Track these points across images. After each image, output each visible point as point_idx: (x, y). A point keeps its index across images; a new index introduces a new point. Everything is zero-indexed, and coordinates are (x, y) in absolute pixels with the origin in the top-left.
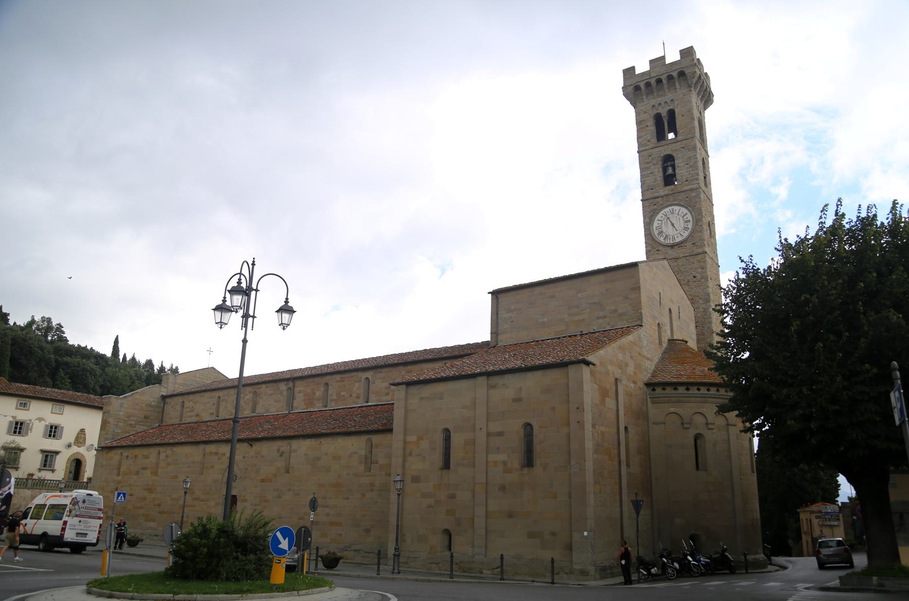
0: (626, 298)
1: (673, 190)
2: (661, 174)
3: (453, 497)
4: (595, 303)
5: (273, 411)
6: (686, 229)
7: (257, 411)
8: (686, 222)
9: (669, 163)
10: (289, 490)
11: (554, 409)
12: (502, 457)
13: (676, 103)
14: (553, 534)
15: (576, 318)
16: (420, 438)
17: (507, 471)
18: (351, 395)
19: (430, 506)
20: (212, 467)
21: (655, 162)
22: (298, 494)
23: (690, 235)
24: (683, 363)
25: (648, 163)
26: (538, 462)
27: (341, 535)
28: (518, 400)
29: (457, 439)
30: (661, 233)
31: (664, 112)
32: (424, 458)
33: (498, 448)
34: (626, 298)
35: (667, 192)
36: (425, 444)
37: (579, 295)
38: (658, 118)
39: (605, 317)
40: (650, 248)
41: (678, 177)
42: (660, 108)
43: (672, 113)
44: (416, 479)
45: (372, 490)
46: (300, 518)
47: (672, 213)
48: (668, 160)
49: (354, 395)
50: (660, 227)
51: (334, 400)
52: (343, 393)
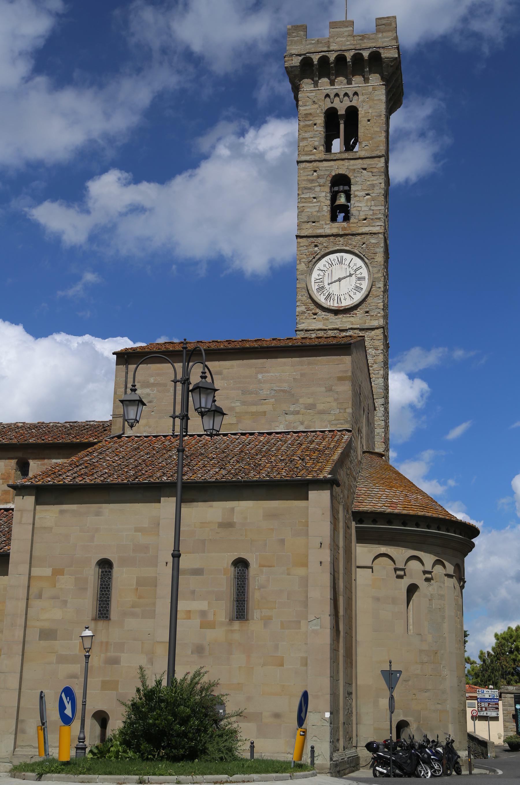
0: (330, 389)
1: (344, 229)
2: (328, 202)
3: (115, 661)
4: (284, 391)
6: (358, 289)
8: (359, 279)
9: (341, 188)
12: (203, 605)
13: (361, 98)
14: (277, 716)
15: (253, 409)
16: (58, 572)
17: (206, 625)
21: (322, 181)
24: (391, 487)
25: (312, 181)
26: (256, 613)
28: (227, 525)
29: (121, 576)
30: (321, 289)
31: (342, 108)
32: (65, 602)
33: (193, 592)
34: (330, 389)
35: (335, 231)
36: (66, 582)
37: (260, 376)
38: (331, 116)
39: (298, 413)
42: (337, 99)
44: (47, 634)
47: (341, 262)
48: (341, 183)
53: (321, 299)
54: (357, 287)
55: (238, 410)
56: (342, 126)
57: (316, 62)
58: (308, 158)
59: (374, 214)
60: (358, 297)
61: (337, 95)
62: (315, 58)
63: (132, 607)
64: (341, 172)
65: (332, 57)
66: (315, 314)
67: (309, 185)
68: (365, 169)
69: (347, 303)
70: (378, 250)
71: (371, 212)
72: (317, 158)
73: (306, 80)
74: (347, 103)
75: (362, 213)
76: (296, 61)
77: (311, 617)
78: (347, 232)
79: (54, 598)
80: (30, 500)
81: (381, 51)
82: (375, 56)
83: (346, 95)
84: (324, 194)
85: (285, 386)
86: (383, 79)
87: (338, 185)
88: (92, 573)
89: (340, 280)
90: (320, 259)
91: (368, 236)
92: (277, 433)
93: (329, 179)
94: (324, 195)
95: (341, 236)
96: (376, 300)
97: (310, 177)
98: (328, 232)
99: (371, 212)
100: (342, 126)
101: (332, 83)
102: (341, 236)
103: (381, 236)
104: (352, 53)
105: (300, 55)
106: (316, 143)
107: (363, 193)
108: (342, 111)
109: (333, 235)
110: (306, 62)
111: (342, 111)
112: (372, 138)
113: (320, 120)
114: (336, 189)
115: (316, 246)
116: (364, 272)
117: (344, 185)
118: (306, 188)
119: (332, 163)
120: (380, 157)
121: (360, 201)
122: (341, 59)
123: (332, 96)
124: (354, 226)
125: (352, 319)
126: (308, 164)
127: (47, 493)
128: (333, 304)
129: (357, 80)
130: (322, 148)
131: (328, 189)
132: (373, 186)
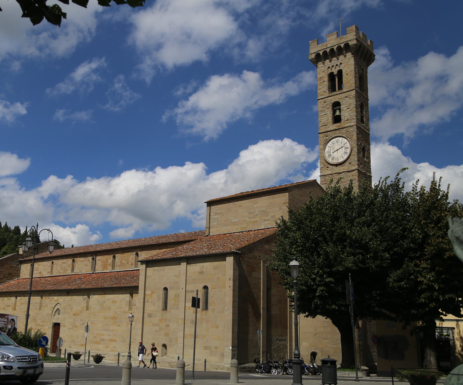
1: (338, 126)
2: (331, 115)
3: (168, 326)
4: (263, 211)
5: (84, 272)
6: (346, 153)
7: (75, 271)
8: (346, 148)
9: (337, 107)
11: (219, 278)
13: (343, 65)
14: (216, 348)
15: (253, 220)
16: (153, 293)
18: (128, 263)
19: (157, 331)
20: (47, 306)
21: (328, 106)
22: (93, 323)
23: (348, 158)
26: (210, 307)
27: (116, 347)
28: (201, 273)
29: (171, 293)
31: (335, 71)
32: (154, 304)
35: (334, 128)
36: (155, 296)
37: (255, 206)
38: (331, 76)
39: (269, 220)
40: (322, 166)
41: (342, 117)
42: (333, 68)
43: (340, 72)
44: (150, 316)
46: (95, 337)
47: (338, 142)
48: (336, 105)
49: (130, 263)
50: (329, 152)
51: (119, 266)
52: (124, 262)
53: (330, 160)
54: (345, 152)
55: (247, 221)
56: (337, 80)
57: (321, 54)
58: (321, 97)
59: (351, 117)
60: (346, 157)
61: (333, 66)
62: (321, 53)
63: (173, 305)
64: (336, 100)
65: (328, 50)
66: (328, 167)
67: (323, 109)
68: (346, 97)
69: (341, 160)
70: (354, 133)
71: (350, 116)
72: (325, 96)
73: (320, 63)
74: (338, 68)
75: (346, 118)
76: (313, 56)
77: (226, 309)
78: (339, 128)
79: (152, 302)
80: (144, 266)
81: (349, 42)
82: (347, 45)
83: (337, 65)
84: (329, 112)
85: (264, 209)
86: (352, 54)
87: (336, 106)
88: (162, 292)
89: (337, 150)
90: (328, 142)
91: (349, 128)
92: (261, 229)
93: (331, 105)
94: (329, 113)
95: (337, 130)
96: (354, 157)
97: (323, 106)
98: (332, 129)
99: (350, 116)
100: (337, 80)
101: (331, 61)
102: (337, 130)
103: (355, 127)
104: (336, 46)
105: (315, 53)
106: (325, 90)
107: (346, 108)
108: (335, 73)
109: (333, 130)
110: (318, 55)
111: (335, 73)
112: (349, 82)
113: (326, 79)
114: (335, 108)
115: (327, 136)
116: (348, 145)
117: (338, 106)
118: (321, 111)
119: (332, 97)
120: (353, 90)
121: (345, 112)
122: (332, 50)
123: (331, 67)
124: (343, 124)
125: (344, 168)
126: (322, 100)
127: (149, 263)
128: (335, 162)
129: (341, 57)
130: (327, 91)
131: (331, 109)
132: (350, 104)
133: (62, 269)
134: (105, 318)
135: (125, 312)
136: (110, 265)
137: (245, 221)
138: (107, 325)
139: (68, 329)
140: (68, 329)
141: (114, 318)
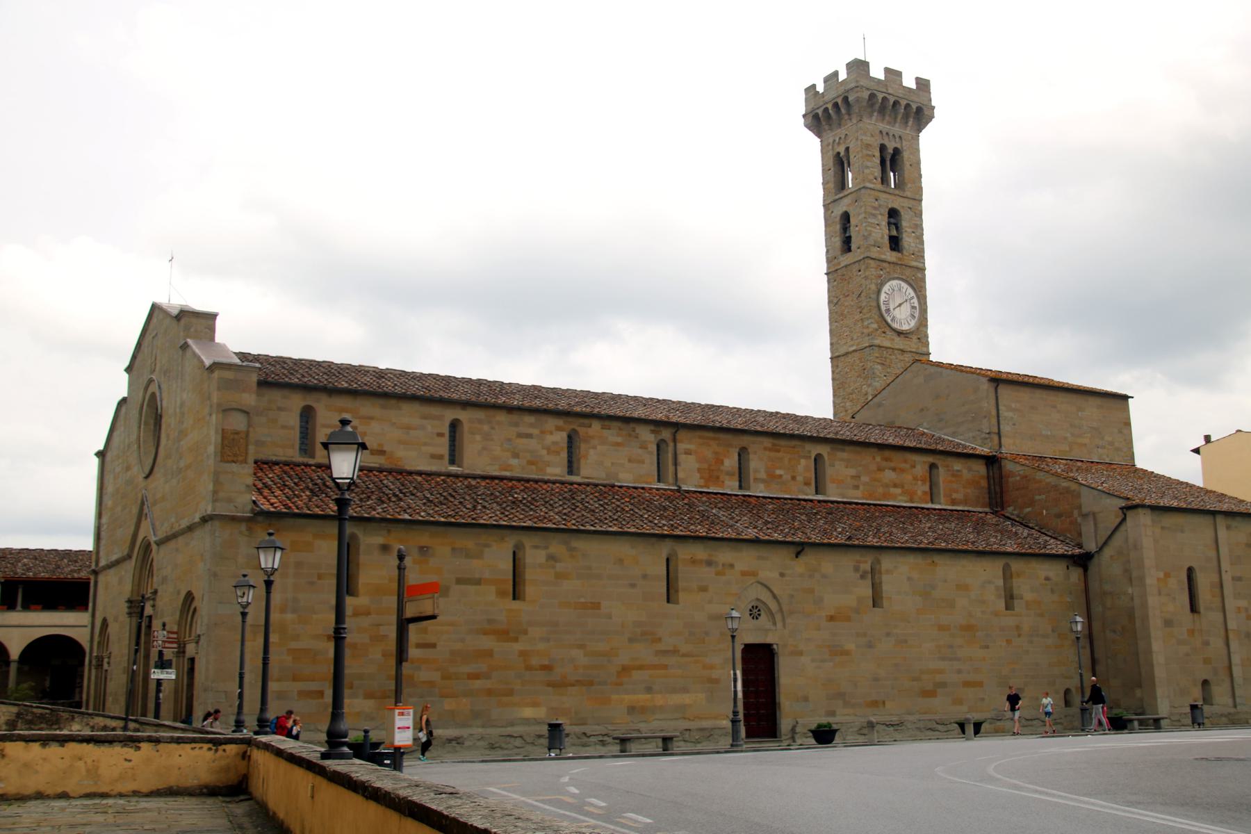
10: (888, 634)
18: (794, 478)
19: (1187, 655)
27: (983, 699)
31: (890, 147)
45: (1019, 636)
46: (914, 679)
49: (800, 479)
51: (763, 481)
52: (778, 472)
133: (516, 455)
134: (941, 628)
135: (996, 614)
136: (730, 474)
137: (1066, 438)
138: (951, 647)
139: (813, 661)
140: (813, 661)
141: (969, 628)
